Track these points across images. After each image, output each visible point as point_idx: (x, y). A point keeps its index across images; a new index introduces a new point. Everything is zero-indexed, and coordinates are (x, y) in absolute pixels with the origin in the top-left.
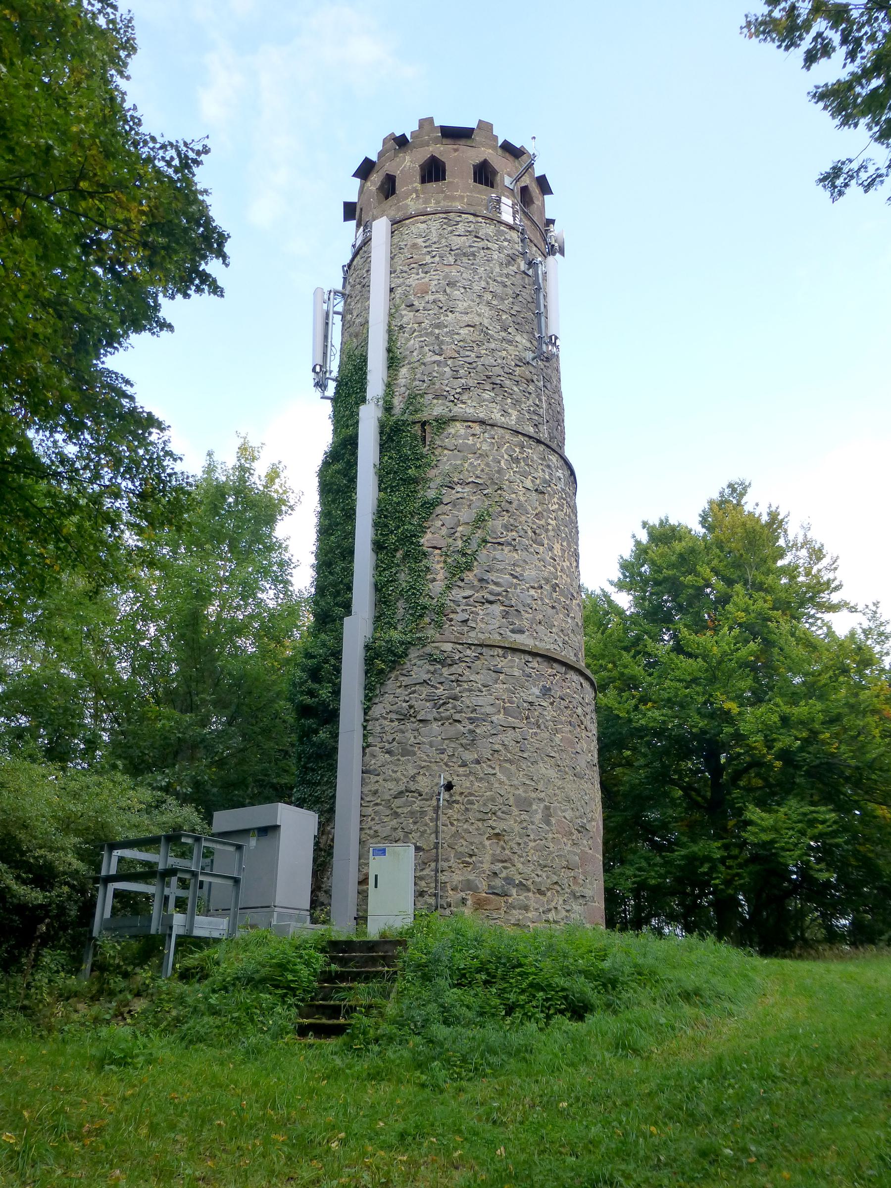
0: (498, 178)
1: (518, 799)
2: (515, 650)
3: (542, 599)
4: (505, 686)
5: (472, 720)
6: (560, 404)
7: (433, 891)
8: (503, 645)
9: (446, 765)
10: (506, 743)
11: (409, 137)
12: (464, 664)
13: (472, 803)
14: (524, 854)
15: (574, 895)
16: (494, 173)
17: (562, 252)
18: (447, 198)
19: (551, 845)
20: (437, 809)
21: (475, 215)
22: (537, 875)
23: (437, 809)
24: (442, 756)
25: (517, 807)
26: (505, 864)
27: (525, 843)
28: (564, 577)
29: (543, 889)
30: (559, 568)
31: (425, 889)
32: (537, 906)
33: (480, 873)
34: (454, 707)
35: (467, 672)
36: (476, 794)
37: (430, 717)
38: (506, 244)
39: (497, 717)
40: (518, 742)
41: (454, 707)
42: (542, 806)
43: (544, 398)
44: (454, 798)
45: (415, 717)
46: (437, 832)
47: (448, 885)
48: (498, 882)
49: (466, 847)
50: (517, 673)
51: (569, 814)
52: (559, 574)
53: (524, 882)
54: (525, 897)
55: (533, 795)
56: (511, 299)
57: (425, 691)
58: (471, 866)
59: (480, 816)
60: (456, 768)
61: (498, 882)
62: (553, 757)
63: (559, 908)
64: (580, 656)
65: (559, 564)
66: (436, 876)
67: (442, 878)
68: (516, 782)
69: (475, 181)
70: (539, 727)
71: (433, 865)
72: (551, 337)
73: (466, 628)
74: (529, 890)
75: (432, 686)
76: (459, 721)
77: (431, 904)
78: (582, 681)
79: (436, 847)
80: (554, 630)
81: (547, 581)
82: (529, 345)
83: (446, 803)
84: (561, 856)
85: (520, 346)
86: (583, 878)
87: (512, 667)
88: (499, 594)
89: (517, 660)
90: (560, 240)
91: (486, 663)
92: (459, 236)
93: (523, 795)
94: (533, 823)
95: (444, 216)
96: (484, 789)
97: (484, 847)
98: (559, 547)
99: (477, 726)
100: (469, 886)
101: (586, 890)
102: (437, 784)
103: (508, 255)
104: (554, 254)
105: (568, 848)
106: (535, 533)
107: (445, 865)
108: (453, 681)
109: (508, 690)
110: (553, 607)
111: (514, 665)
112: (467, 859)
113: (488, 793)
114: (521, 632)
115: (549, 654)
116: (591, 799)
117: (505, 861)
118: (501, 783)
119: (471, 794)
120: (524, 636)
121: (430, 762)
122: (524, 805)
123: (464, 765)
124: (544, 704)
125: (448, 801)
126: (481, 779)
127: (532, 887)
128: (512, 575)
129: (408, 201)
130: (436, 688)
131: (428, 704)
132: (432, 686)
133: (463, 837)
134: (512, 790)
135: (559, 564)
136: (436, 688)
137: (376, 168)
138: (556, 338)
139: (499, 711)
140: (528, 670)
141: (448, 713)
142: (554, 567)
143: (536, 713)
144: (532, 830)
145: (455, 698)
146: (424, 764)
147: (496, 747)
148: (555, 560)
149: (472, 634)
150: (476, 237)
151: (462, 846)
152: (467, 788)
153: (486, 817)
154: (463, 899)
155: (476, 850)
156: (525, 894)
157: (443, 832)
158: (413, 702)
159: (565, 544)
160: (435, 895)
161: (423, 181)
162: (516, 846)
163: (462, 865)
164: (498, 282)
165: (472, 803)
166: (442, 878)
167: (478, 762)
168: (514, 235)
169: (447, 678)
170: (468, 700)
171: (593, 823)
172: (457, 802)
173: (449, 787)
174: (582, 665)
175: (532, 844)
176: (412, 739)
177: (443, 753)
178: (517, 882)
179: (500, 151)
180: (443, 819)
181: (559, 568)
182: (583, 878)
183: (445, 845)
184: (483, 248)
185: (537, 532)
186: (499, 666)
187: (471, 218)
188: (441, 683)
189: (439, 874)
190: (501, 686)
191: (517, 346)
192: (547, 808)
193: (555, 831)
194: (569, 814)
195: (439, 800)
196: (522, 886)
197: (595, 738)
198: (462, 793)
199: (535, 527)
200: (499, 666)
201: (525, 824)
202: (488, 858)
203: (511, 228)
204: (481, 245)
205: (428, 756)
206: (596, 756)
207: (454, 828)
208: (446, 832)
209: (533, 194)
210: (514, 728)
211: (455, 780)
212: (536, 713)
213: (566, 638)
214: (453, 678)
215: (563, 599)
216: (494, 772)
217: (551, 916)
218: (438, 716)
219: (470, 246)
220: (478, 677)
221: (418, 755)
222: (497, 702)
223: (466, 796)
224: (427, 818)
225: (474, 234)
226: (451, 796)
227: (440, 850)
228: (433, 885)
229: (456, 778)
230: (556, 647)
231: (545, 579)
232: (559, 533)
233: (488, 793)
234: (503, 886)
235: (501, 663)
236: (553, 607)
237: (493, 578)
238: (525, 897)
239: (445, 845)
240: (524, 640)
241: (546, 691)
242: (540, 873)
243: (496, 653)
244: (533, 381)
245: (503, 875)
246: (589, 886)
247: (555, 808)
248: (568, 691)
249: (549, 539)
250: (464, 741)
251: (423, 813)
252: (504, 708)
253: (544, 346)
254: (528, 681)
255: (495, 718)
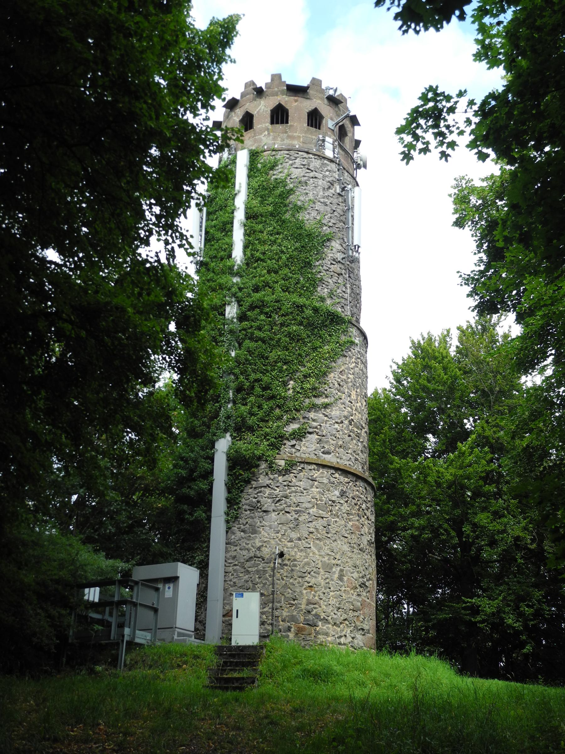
0: (324, 121)
1: (324, 563)
2: (324, 466)
3: (342, 430)
4: (318, 490)
5: (297, 512)
6: (359, 287)
7: (270, 621)
8: (317, 462)
9: (280, 540)
10: (317, 527)
11: (264, 88)
12: (292, 475)
13: (295, 566)
14: (327, 600)
15: (357, 628)
16: (322, 117)
17: (365, 167)
18: (289, 137)
19: (344, 595)
20: (273, 569)
21: (308, 153)
22: (335, 614)
23: (273, 569)
24: (278, 535)
25: (323, 569)
26: (315, 606)
27: (328, 593)
28: (357, 414)
29: (338, 623)
30: (354, 408)
31: (266, 620)
32: (334, 634)
33: (299, 611)
34: (286, 503)
35: (294, 480)
36: (298, 560)
37: (271, 509)
38: (327, 173)
39: (312, 510)
40: (325, 527)
41: (286, 503)
42: (338, 569)
43: (348, 286)
44: (284, 562)
45: (261, 509)
46: (273, 584)
47: (280, 619)
48: (310, 617)
49: (292, 594)
50: (325, 481)
51: (356, 575)
52: (354, 412)
53: (326, 618)
54: (327, 627)
55: (334, 562)
56: (329, 215)
57: (268, 491)
58: (294, 606)
59: (300, 574)
60: (286, 543)
61: (310, 617)
62: (346, 537)
63: (347, 635)
64: (365, 468)
65: (354, 406)
66: (272, 612)
67: (276, 613)
68: (323, 553)
69: (308, 125)
70: (338, 517)
71: (271, 605)
72: (355, 246)
73: (294, 450)
74: (329, 623)
75: (272, 488)
76: (288, 512)
77: (269, 630)
78: (366, 486)
79: (273, 594)
80: (349, 452)
81: (346, 418)
82: (340, 248)
83: (279, 565)
84: (349, 602)
85: (334, 249)
86: (363, 617)
87: (322, 477)
88: (316, 428)
89: (326, 473)
90: (364, 159)
91: (306, 474)
92: (297, 168)
93: (327, 561)
94: (332, 580)
95: (287, 152)
96: (303, 557)
97: (302, 594)
98: (355, 393)
99: (300, 516)
100: (293, 619)
101: (364, 626)
102: (274, 553)
103: (329, 182)
104: (360, 168)
105: (354, 597)
106: (339, 385)
107: (279, 605)
108: (285, 486)
109: (319, 492)
110: (349, 436)
111: (323, 475)
112: (292, 602)
113: (306, 560)
114: (329, 453)
115: (346, 469)
116: (369, 565)
117: (315, 604)
118: (314, 553)
119: (295, 560)
120: (330, 456)
121: (270, 539)
122: (328, 568)
123: (291, 541)
124: (342, 502)
125: (280, 564)
126: (302, 550)
127: (331, 621)
128: (324, 414)
129: (262, 136)
130: (275, 490)
131: (269, 500)
132: (272, 488)
133: (289, 588)
134: (321, 558)
135: (354, 406)
136: (275, 490)
137: (240, 105)
138: (359, 247)
139: (314, 506)
140: (332, 479)
141: (282, 507)
142: (351, 408)
143: (337, 508)
144: (332, 584)
145: (286, 497)
146: (266, 539)
147: (311, 530)
148: (352, 403)
149: (298, 454)
150: (308, 169)
151: (289, 593)
152: (292, 556)
153: (304, 575)
154: (289, 627)
155: (297, 596)
156: (327, 626)
157: (277, 584)
158: (260, 499)
159: (358, 390)
160: (272, 624)
161: (272, 123)
162: (322, 595)
163: (288, 606)
164: (321, 203)
165: (295, 566)
166: (276, 613)
167: (299, 539)
168: (333, 166)
169: (281, 483)
170: (294, 499)
171: (371, 582)
172: (286, 565)
173: (281, 555)
174: (367, 475)
175: (332, 594)
176: (259, 523)
177: (278, 533)
178: (322, 617)
179: (326, 101)
180: (278, 575)
181: (354, 408)
182: (363, 617)
183: (278, 593)
184: (312, 178)
185: (341, 384)
186: (315, 476)
187: (305, 155)
188: (278, 487)
189: (275, 611)
190: (315, 489)
191: (332, 250)
192: (341, 571)
193: (346, 586)
194: (356, 575)
195: (275, 563)
196: (325, 621)
197: (373, 525)
198: (289, 560)
199: (339, 380)
200: (315, 476)
201: (328, 581)
202: (304, 601)
203: (331, 161)
204: (312, 174)
205: (268, 534)
206: (374, 536)
207: (284, 582)
208: (280, 584)
209: (347, 129)
210: (322, 518)
211: (285, 550)
212: (337, 508)
213: (357, 457)
214: (285, 483)
215: (356, 430)
216: (309, 546)
217: (343, 640)
218: (275, 509)
219: (304, 176)
220: (301, 483)
221: (262, 534)
222: (313, 500)
223: (292, 561)
224: (267, 575)
225: (306, 167)
226: (283, 561)
227: (275, 596)
228: (270, 618)
229: (285, 549)
230: (350, 463)
231: (344, 416)
232: (355, 383)
233: (306, 560)
234: (313, 620)
235: (316, 474)
236: (349, 436)
237: (312, 416)
238: (327, 627)
239: (278, 593)
240: (330, 459)
241: (343, 494)
242: (336, 612)
243: (313, 468)
244: (342, 274)
245: (313, 613)
246: (366, 623)
247: (346, 571)
248: (357, 493)
249: (348, 389)
250: (292, 526)
251: (265, 572)
252: (317, 504)
253: (350, 252)
254: (332, 487)
255: (311, 511)
